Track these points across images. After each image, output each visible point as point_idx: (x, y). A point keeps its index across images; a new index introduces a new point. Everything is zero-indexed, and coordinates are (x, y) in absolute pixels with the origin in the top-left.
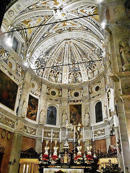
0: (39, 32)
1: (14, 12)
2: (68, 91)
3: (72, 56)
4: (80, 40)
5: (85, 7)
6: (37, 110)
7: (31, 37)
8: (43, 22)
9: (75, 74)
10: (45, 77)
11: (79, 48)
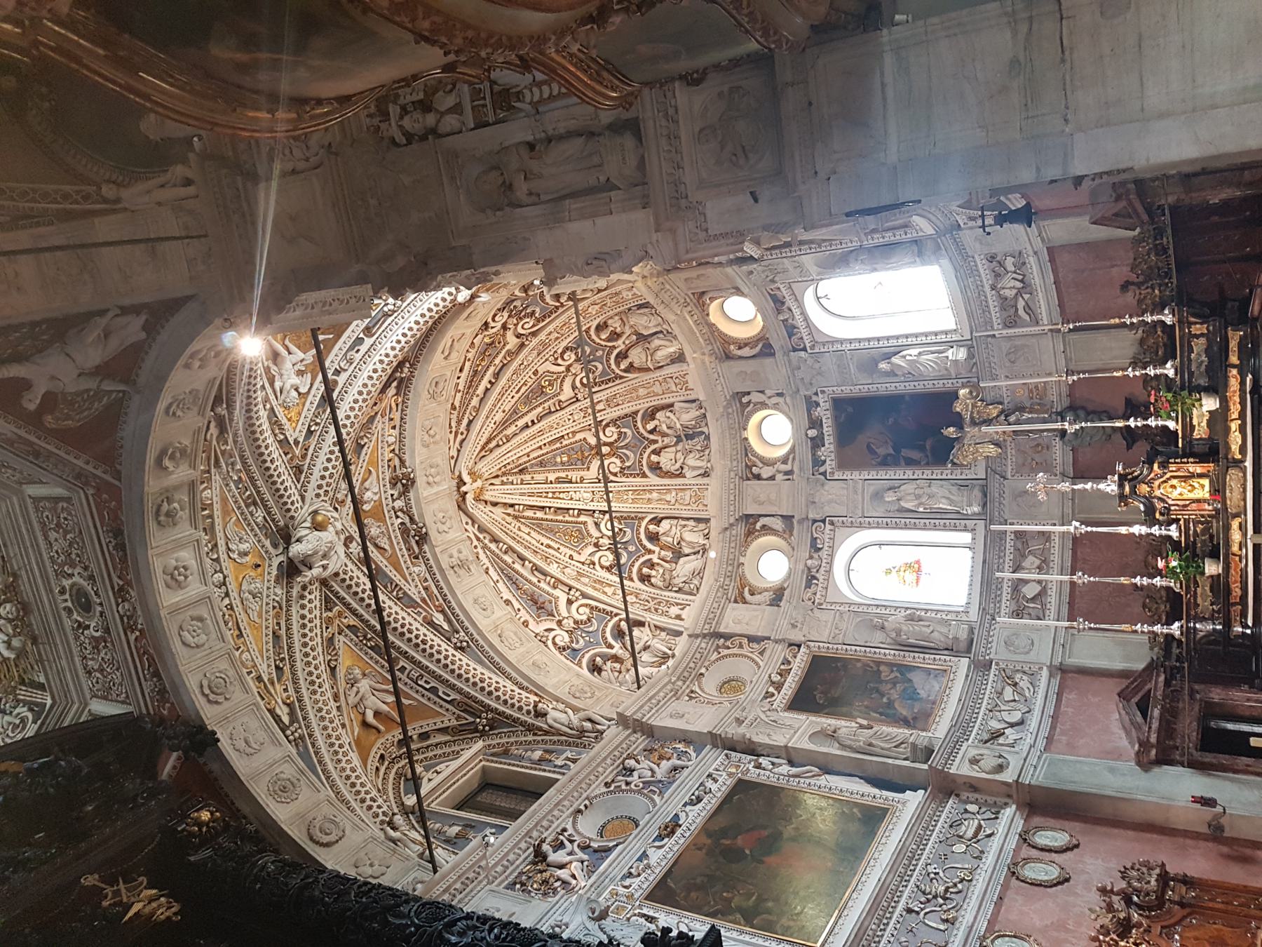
0: (418, 657)
2: (758, 477)
3: (555, 464)
4: (459, 422)
5: (272, 397)
6: (878, 663)
9: (656, 442)
10: (679, 617)
11: (505, 424)
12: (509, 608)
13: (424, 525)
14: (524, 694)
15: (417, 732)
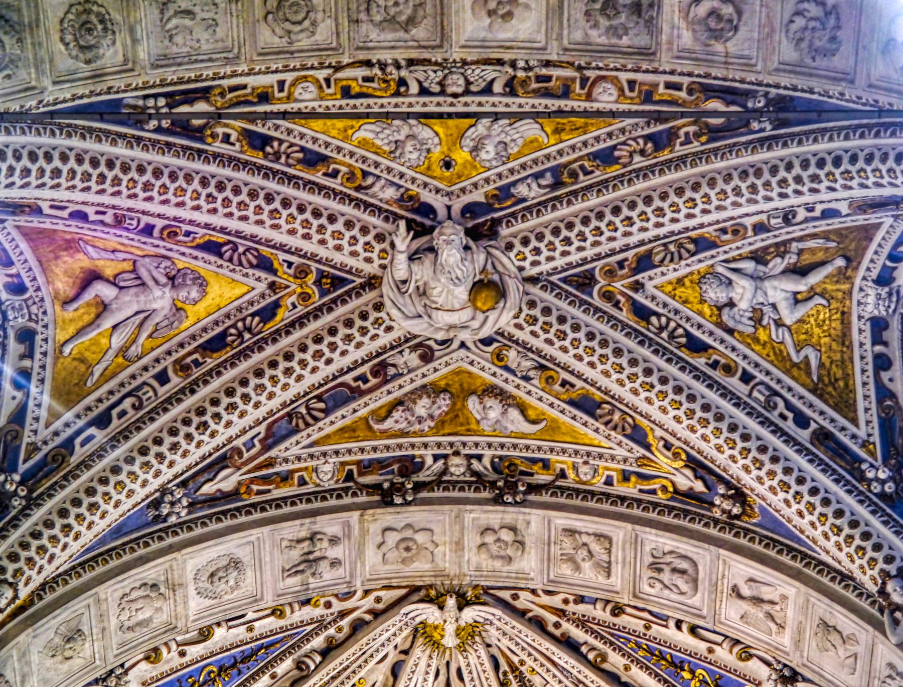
0: (177, 410)
4: (582, 622)
8: (249, 330)
12: (193, 634)
13: (407, 504)
15: (36, 369)
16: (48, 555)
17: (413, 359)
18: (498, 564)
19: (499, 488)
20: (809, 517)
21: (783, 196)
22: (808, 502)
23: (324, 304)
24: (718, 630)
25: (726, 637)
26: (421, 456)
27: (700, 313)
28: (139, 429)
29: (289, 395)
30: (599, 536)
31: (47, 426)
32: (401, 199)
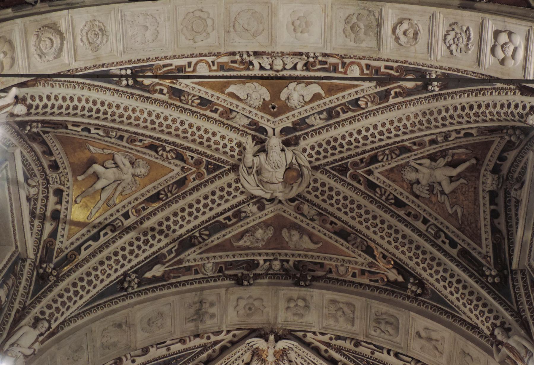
1: (62, 44)
7: (78, 249)
13: (250, 285)
14: (61, 319)
15: (63, 210)
16: (66, 307)
17: (254, 209)
18: (296, 318)
19: (297, 278)
20: (456, 295)
21: (444, 125)
22: (456, 287)
23: (209, 179)
24: (409, 355)
25: (413, 358)
26: (257, 260)
27: (402, 187)
28: (114, 242)
29: (190, 226)
30: (349, 304)
31: (68, 239)
32: (250, 124)
